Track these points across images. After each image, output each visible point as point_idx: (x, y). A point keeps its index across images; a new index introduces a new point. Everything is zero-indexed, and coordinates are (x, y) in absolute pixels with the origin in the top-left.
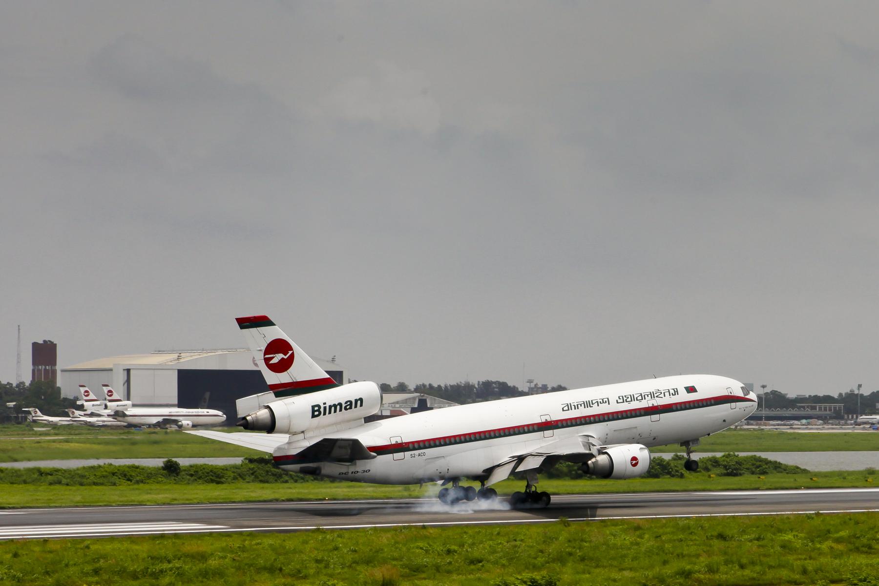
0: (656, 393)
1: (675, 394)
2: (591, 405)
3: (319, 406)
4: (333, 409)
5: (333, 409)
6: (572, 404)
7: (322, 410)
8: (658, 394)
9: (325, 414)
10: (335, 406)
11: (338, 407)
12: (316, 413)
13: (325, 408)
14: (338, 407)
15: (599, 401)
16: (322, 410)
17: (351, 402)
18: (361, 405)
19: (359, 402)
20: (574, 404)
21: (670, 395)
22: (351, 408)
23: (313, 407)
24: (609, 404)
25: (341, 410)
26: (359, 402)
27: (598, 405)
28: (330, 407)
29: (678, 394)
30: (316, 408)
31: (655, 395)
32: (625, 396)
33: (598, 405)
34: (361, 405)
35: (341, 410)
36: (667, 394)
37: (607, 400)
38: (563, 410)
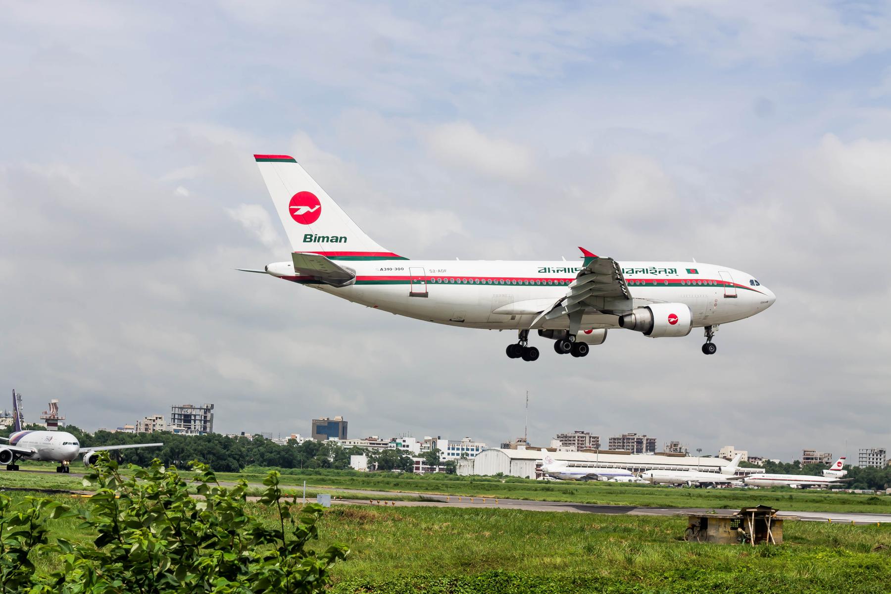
3: (312, 236)
4: (321, 239)
5: (321, 239)
7: (313, 238)
9: (315, 241)
11: (326, 239)
12: (307, 240)
13: (316, 237)
14: (326, 239)
16: (313, 238)
17: (337, 238)
18: (345, 242)
19: (343, 240)
22: (336, 241)
23: (306, 235)
25: (327, 241)
26: (343, 240)
28: (319, 237)
30: (308, 237)
34: (345, 242)
35: (327, 241)
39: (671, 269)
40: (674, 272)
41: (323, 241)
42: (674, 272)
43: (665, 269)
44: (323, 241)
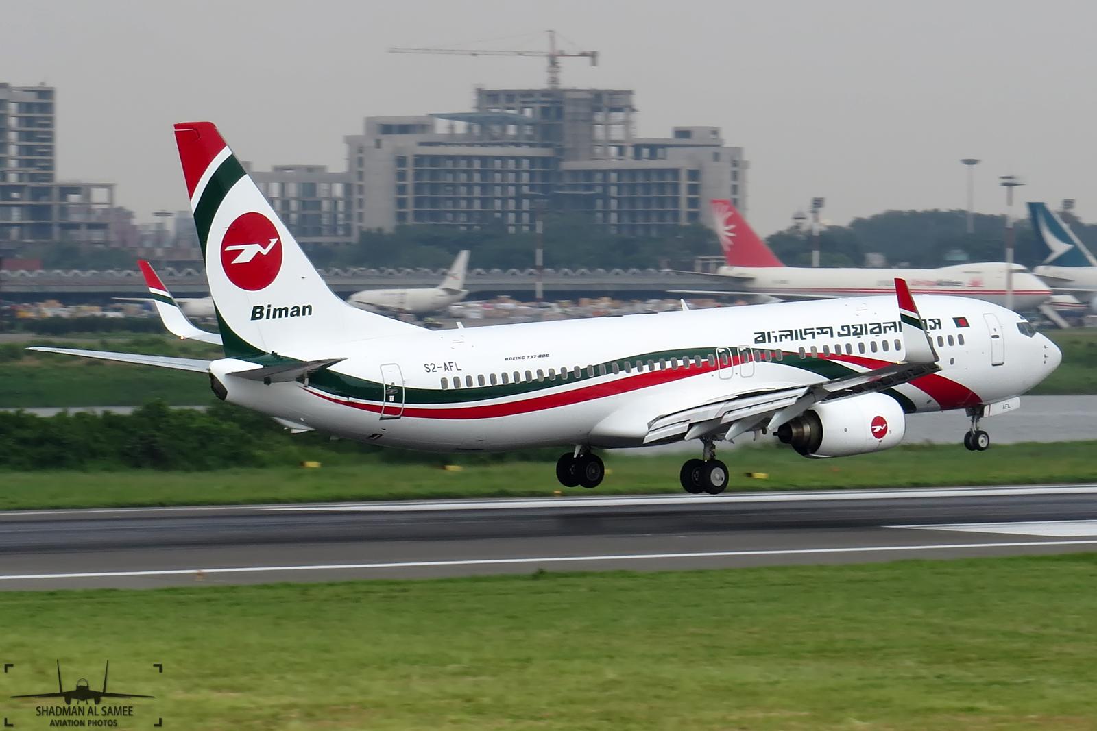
1: (934, 328)
2: (804, 336)
4: (278, 312)
5: (278, 312)
6: (772, 335)
10: (280, 310)
15: (816, 331)
20: (774, 334)
24: (832, 336)
27: (814, 337)
28: (275, 310)
29: (940, 327)
32: (853, 326)
33: (814, 337)
37: (828, 330)
38: (756, 341)
40: (937, 326)
41: (280, 316)
42: (937, 326)
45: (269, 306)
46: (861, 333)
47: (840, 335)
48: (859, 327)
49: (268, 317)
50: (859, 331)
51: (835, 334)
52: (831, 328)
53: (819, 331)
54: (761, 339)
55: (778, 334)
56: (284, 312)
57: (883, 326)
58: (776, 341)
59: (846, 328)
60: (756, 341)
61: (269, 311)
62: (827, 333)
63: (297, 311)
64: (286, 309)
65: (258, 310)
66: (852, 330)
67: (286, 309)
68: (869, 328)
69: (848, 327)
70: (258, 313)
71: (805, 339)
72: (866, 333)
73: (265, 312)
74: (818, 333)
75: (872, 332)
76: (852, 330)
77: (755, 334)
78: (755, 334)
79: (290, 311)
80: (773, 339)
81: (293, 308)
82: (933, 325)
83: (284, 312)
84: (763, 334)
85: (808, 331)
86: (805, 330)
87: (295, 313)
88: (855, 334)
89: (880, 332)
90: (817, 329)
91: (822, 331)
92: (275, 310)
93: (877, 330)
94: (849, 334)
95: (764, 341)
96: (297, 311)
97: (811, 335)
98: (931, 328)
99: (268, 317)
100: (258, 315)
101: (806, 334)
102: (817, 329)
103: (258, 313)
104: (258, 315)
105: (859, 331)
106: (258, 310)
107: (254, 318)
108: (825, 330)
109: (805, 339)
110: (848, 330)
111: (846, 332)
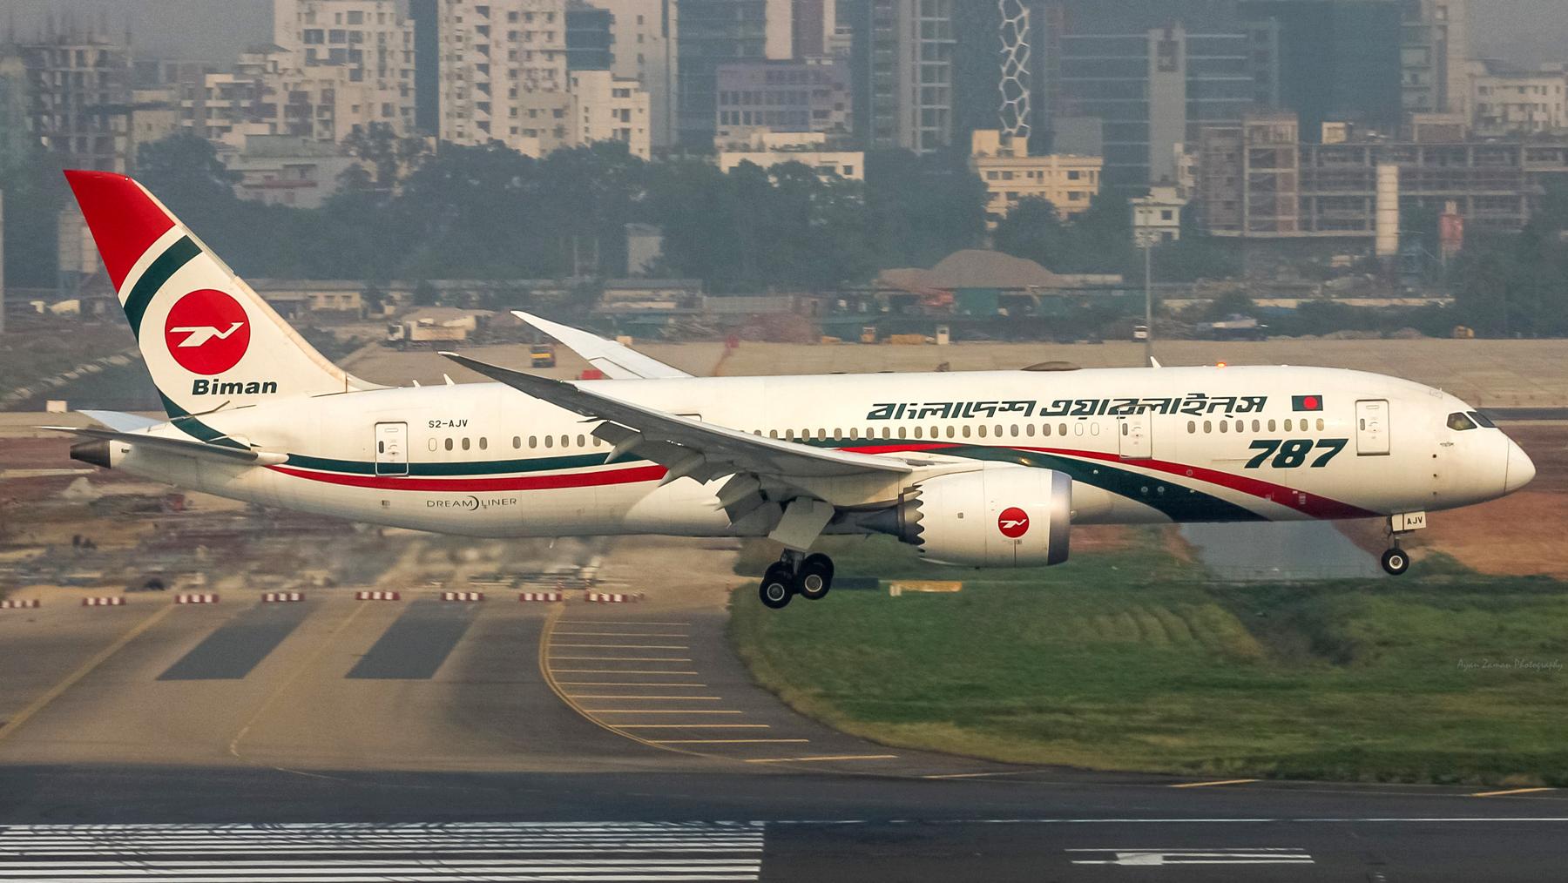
0: (1187, 404)
1: (1248, 410)
2: (971, 413)
4: (228, 388)
5: (228, 388)
6: (908, 407)
8: (1192, 406)
10: (232, 386)
20: (913, 408)
21: (1229, 410)
24: (1028, 414)
27: (990, 415)
28: (224, 386)
29: (1259, 410)
31: (1181, 407)
32: (1078, 402)
36: (1220, 410)
37: (1026, 406)
38: (872, 416)
39: (1250, 400)
40: (1255, 407)
41: (231, 392)
42: (1255, 407)
43: (1233, 400)
44: (231, 392)
45: (217, 380)
46: (1091, 412)
47: (1044, 413)
48: (1089, 404)
49: (214, 392)
50: (1087, 409)
51: (1037, 410)
52: (1032, 404)
53: (1007, 406)
54: (884, 413)
55: (918, 409)
56: (236, 388)
57: (1139, 403)
58: (912, 417)
59: (1062, 405)
60: (872, 416)
61: (215, 386)
62: (1021, 409)
63: (254, 388)
64: (240, 386)
65: (201, 384)
66: (1074, 407)
67: (240, 386)
68: (1111, 405)
69: (1069, 403)
70: (201, 387)
71: (973, 416)
72: (1101, 413)
73: (210, 387)
74: (1002, 409)
75: (1114, 411)
76: (1074, 407)
77: (875, 405)
78: (875, 405)
79: (245, 387)
80: (906, 414)
81: (249, 385)
82: (1245, 404)
83: (236, 388)
84: (890, 407)
85: (983, 406)
86: (979, 404)
87: (252, 390)
88: (1073, 413)
89: (1131, 411)
90: (1003, 403)
91: (1012, 406)
92: (224, 386)
93: (1126, 409)
94: (1064, 413)
95: (887, 417)
96: (254, 388)
97: (987, 411)
98: (1240, 409)
99: (214, 392)
100: (201, 390)
101: (978, 408)
102: (1003, 403)
103: (201, 387)
104: (201, 390)
105: (1084, 410)
106: (201, 384)
107: (195, 392)
108: (1017, 406)
109: (973, 416)
110: (1064, 408)
111: (1060, 410)
